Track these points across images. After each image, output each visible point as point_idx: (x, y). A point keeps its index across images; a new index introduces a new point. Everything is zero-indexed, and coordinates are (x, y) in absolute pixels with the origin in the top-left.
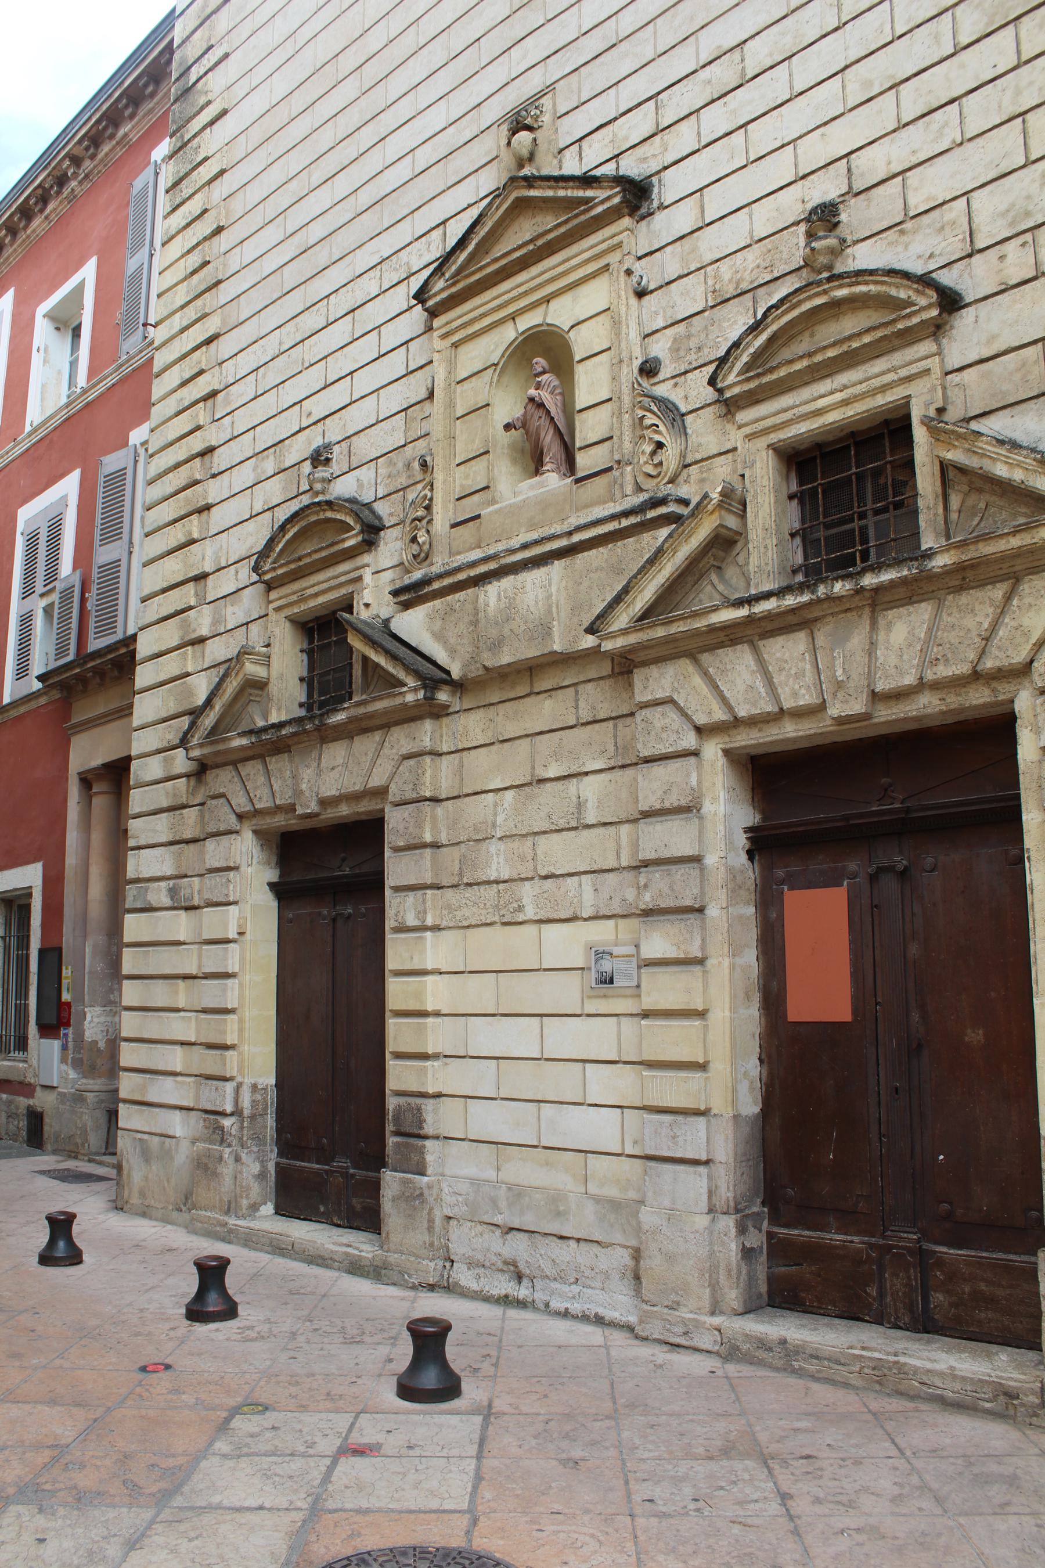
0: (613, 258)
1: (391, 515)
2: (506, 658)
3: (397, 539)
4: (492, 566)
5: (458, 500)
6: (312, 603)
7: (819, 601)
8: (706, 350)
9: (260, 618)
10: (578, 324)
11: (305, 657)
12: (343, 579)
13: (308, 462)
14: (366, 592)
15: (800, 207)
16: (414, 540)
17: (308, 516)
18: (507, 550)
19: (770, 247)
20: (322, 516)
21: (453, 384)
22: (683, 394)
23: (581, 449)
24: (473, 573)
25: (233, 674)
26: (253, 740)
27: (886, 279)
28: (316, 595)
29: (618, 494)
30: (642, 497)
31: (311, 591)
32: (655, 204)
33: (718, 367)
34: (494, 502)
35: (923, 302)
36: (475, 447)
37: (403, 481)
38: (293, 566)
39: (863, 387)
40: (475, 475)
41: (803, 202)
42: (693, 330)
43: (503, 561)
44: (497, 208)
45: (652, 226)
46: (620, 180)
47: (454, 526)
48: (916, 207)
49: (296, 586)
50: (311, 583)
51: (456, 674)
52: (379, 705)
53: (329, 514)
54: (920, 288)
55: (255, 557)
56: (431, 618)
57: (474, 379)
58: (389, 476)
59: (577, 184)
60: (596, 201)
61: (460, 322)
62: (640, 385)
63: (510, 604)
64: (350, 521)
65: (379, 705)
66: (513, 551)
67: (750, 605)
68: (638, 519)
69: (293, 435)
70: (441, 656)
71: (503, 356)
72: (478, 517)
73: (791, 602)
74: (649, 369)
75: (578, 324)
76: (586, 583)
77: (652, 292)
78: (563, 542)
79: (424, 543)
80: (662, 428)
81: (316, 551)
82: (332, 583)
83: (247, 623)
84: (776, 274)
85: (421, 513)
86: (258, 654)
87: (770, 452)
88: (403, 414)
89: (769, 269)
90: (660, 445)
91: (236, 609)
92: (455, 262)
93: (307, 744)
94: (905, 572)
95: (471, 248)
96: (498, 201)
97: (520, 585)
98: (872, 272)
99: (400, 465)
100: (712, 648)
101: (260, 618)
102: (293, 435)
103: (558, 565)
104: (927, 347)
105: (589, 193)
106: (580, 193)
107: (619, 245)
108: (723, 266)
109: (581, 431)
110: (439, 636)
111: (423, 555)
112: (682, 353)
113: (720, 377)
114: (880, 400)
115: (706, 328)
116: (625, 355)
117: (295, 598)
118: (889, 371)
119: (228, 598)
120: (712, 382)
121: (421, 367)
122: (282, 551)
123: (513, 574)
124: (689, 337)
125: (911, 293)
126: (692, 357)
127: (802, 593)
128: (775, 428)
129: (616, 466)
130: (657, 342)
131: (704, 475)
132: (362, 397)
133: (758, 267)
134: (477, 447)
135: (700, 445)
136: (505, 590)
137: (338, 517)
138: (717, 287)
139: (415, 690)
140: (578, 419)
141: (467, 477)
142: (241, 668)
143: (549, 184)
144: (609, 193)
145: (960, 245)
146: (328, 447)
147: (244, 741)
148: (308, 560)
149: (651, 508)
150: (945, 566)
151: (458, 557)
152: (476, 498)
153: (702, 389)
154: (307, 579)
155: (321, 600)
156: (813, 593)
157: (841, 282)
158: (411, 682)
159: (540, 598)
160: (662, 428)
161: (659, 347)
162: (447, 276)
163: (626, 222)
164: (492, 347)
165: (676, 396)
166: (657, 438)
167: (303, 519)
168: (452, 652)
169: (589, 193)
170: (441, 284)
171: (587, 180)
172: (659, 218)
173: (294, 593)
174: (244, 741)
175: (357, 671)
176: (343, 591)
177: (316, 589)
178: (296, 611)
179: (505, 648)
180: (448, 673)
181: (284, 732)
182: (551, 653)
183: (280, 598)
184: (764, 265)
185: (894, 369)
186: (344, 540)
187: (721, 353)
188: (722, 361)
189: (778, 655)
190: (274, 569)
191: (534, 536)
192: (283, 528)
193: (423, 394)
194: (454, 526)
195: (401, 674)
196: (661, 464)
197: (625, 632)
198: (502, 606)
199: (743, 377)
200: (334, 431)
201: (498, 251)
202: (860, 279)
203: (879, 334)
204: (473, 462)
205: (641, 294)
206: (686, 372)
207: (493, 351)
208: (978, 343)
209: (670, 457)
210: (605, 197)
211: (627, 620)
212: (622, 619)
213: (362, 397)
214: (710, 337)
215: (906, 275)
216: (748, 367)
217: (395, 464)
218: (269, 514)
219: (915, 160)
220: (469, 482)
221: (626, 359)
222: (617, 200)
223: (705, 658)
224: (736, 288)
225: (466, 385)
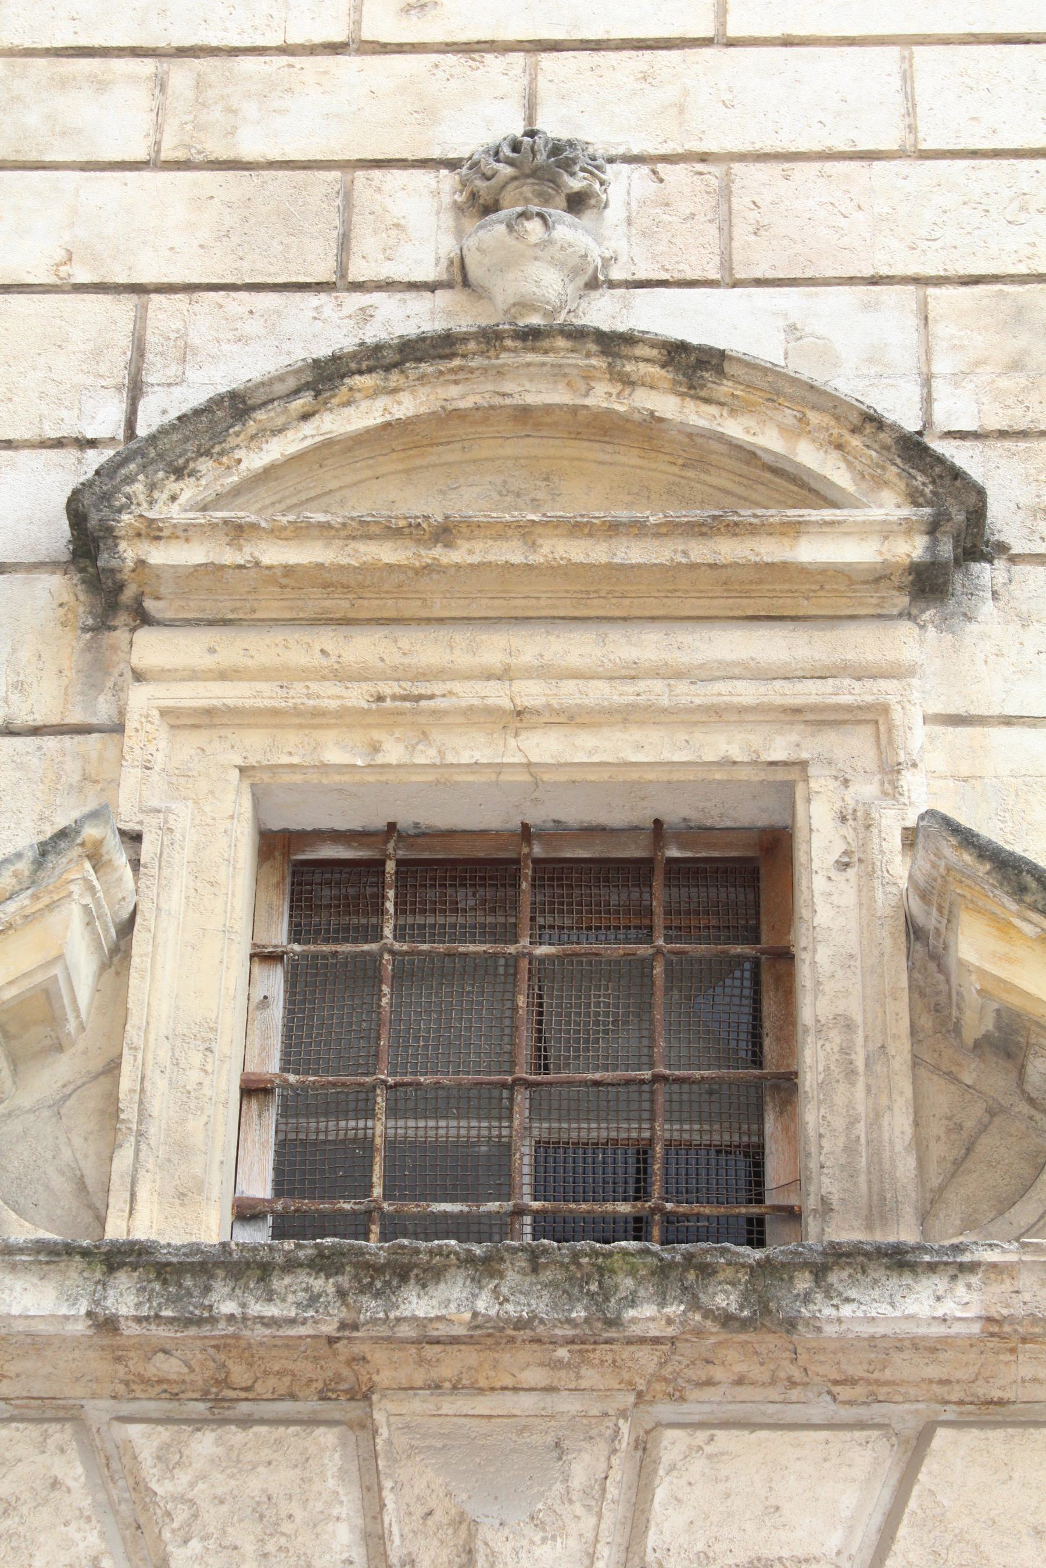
12: (747, 693)
17: (500, 373)
31: (497, 694)
38: (388, 553)
58: (1015, 365)
69: (284, 50)
81: (577, 528)
82: (655, 691)
93: (527, 1402)
102: (284, 50)
117: (357, 696)
122: (269, 473)
132: (787, 42)
137: (734, 428)
142: (28, 918)
148: (512, 552)
154: (461, 637)
167: (457, 376)
173: (342, 675)
178: (334, 755)
183: (223, 676)
186: (795, 529)
190: (238, 531)
213: (787, 42)
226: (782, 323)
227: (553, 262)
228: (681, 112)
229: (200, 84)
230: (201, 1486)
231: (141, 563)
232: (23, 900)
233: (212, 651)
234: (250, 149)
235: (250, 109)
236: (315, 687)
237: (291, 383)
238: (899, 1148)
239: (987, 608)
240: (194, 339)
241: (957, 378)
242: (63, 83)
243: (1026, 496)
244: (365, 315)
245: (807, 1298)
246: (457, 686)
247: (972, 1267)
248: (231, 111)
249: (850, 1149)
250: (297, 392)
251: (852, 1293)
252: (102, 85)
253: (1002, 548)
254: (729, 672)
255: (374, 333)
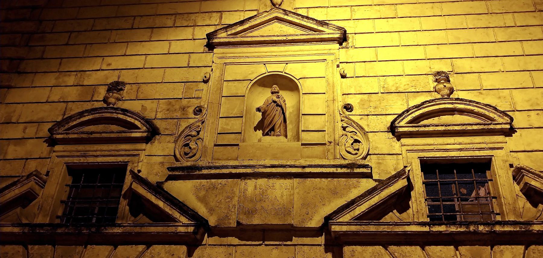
0: (329, 58)
1: (167, 129)
2: (256, 221)
3: (169, 142)
4: (249, 171)
5: (218, 134)
6: (91, 160)
7: (470, 232)
8: (380, 110)
9: (40, 158)
10: (304, 78)
11: (68, 189)
12: (123, 153)
13: (106, 88)
14: (140, 164)
15: (429, 70)
16: (187, 145)
18: (260, 165)
19: (414, 79)
20: (115, 115)
21: (223, 81)
22: (366, 123)
23: (303, 131)
24: (234, 171)
25: (19, 186)
26: (26, 231)
27: (484, 107)
28: (97, 156)
29: (331, 157)
30: (346, 162)
31: (94, 153)
32: (350, 45)
33: (397, 117)
34: (244, 141)
35: (500, 120)
36: (234, 112)
37: (178, 114)
39: (471, 146)
40: (235, 125)
41: (430, 68)
42: (372, 99)
43: (256, 170)
44: (265, 16)
45: (348, 52)
46: (340, 28)
47: (215, 145)
48: (486, 86)
49: (81, 147)
50: (95, 149)
51: (212, 221)
52: (153, 229)
53: (121, 116)
54: (501, 115)
55: (53, 124)
56: (197, 189)
57: (236, 82)
58: (168, 110)
59: (315, 23)
60: (326, 32)
61: (232, 55)
62: (344, 113)
63: (263, 193)
64: (137, 123)
65: (153, 229)
66: (265, 167)
67: (430, 227)
68: (349, 171)
70: (202, 210)
71: (256, 78)
72: (237, 145)
73: (455, 230)
74: (348, 108)
75: (304, 78)
76: (312, 194)
77: (347, 78)
78: (300, 170)
79: (194, 149)
80: (358, 133)
83: (27, 159)
84: (418, 91)
85: (194, 133)
86: (41, 178)
87: (419, 160)
88: (183, 84)
89: (414, 87)
90: (356, 141)
91: (18, 148)
92: (234, 29)
94: (518, 229)
95: (246, 26)
96: (266, 14)
97: (271, 185)
98: (477, 103)
99: (177, 107)
100: (399, 244)
101: (40, 158)
103: (296, 181)
104: (501, 138)
105: (320, 28)
106: (315, 27)
107: (333, 54)
108: (389, 80)
109: (305, 123)
110: (203, 200)
111: (191, 155)
112: (365, 107)
113: (398, 121)
114: (477, 153)
115: (380, 100)
116: (336, 98)
117: (78, 154)
118: (483, 143)
119: (12, 141)
120: (393, 122)
121: (198, 67)
123: (267, 178)
124: (370, 101)
125: (495, 116)
126: (372, 110)
127: (461, 227)
128: (423, 151)
129: (328, 144)
130: (350, 98)
131: (380, 161)
132: (152, 68)
133: (408, 85)
134: (235, 112)
135: (377, 147)
136: (261, 185)
138: (386, 86)
139: (187, 226)
140: (303, 119)
141: (228, 124)
143: (298, 17)
144: (332, 32)
145: (509, 106)
146: (124, 84)
147: (16, 230)
148: (98, 135)
149: (357, 168)
150: (539, 231)
151: (220, 162)
152: (233, 136)
153: (377, 124)
155: (100, 160)
156: (467, 228)
157: (461, 102)
158: (184, 220)
159: (285, 194)
160: (358, 133)
161: (352, 100)
162: (229, 33)
163: (337, 46)
164: (250, 72)
165: (363, 123)
166: (356, 137)
168: (211, 211)
169: (320, 28)
170: (224, 35)
171: (322, 23)
172: (351, 51)
174: (16, 230)
175: (124, 205)
176: (120, 159)
177: (98, 153)
179: (256, 215)
180: (207, 221)
181: (59, 231)
182: (289, 224)
184: (412, 85)
185: (486, 143)
186: (132, 132)
187: (400, 112)
188: (400, 115)
189: (438, 254)
190: (67, 134)
191: (276, 163)
192: (81, 114)
193: (200, 79)
194: (215, 145)
195: (176, 214)
196: (358, 150)
197: (348, 224)
198: (257, 192)
199: (411, 125)
200: (126, 77)
201: (255, 33)
202: (471, 103)
203: (481, 127)
204: (232, 119)
205: (343, 76)
206: (368, 115)
207: (250, 74)
208: (523, 144)
209: (363, 148)
210: (329, 32)
211: (349, 218)
212: (347, 217)
214: (382, 104)
215: (495, 109)
216: (410, 122)
217: (173, 105)
218: (64, 105)
219: (483, 70)
220: (229, 128)
221: (337, 101)
222: (337, 36)
223: (392, 248)
224: (396, 89)
225: (230, 83)
226: (141, 105)
227: (114, 98)
228: (136, 78)
229: (81, 75)
230: (35, 252)
231: (56, 138)
232: (26, 181)
233: (63, 148)
234: (86, 83)
235: (86, 78)
236: (74, 153)
237: (77, 115)
238: (127, 210)
239: (156, 141)
240: (72, 108)
241: (160, 112)
242: (65, 76)
243: (164, 127)
244: (93, 105)
245: (103, 230)
246: (90, 152)
247: (122, 226)
248: (84, 79)
249: (122, 210)
250: (77, 116)
251: (108, 229)
252: (70, 75)
253: (161, 133)
254: (122, 150)
255: (94, 107)
